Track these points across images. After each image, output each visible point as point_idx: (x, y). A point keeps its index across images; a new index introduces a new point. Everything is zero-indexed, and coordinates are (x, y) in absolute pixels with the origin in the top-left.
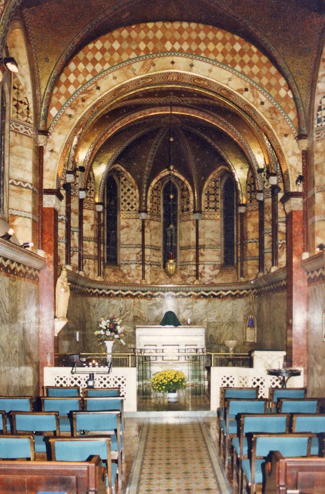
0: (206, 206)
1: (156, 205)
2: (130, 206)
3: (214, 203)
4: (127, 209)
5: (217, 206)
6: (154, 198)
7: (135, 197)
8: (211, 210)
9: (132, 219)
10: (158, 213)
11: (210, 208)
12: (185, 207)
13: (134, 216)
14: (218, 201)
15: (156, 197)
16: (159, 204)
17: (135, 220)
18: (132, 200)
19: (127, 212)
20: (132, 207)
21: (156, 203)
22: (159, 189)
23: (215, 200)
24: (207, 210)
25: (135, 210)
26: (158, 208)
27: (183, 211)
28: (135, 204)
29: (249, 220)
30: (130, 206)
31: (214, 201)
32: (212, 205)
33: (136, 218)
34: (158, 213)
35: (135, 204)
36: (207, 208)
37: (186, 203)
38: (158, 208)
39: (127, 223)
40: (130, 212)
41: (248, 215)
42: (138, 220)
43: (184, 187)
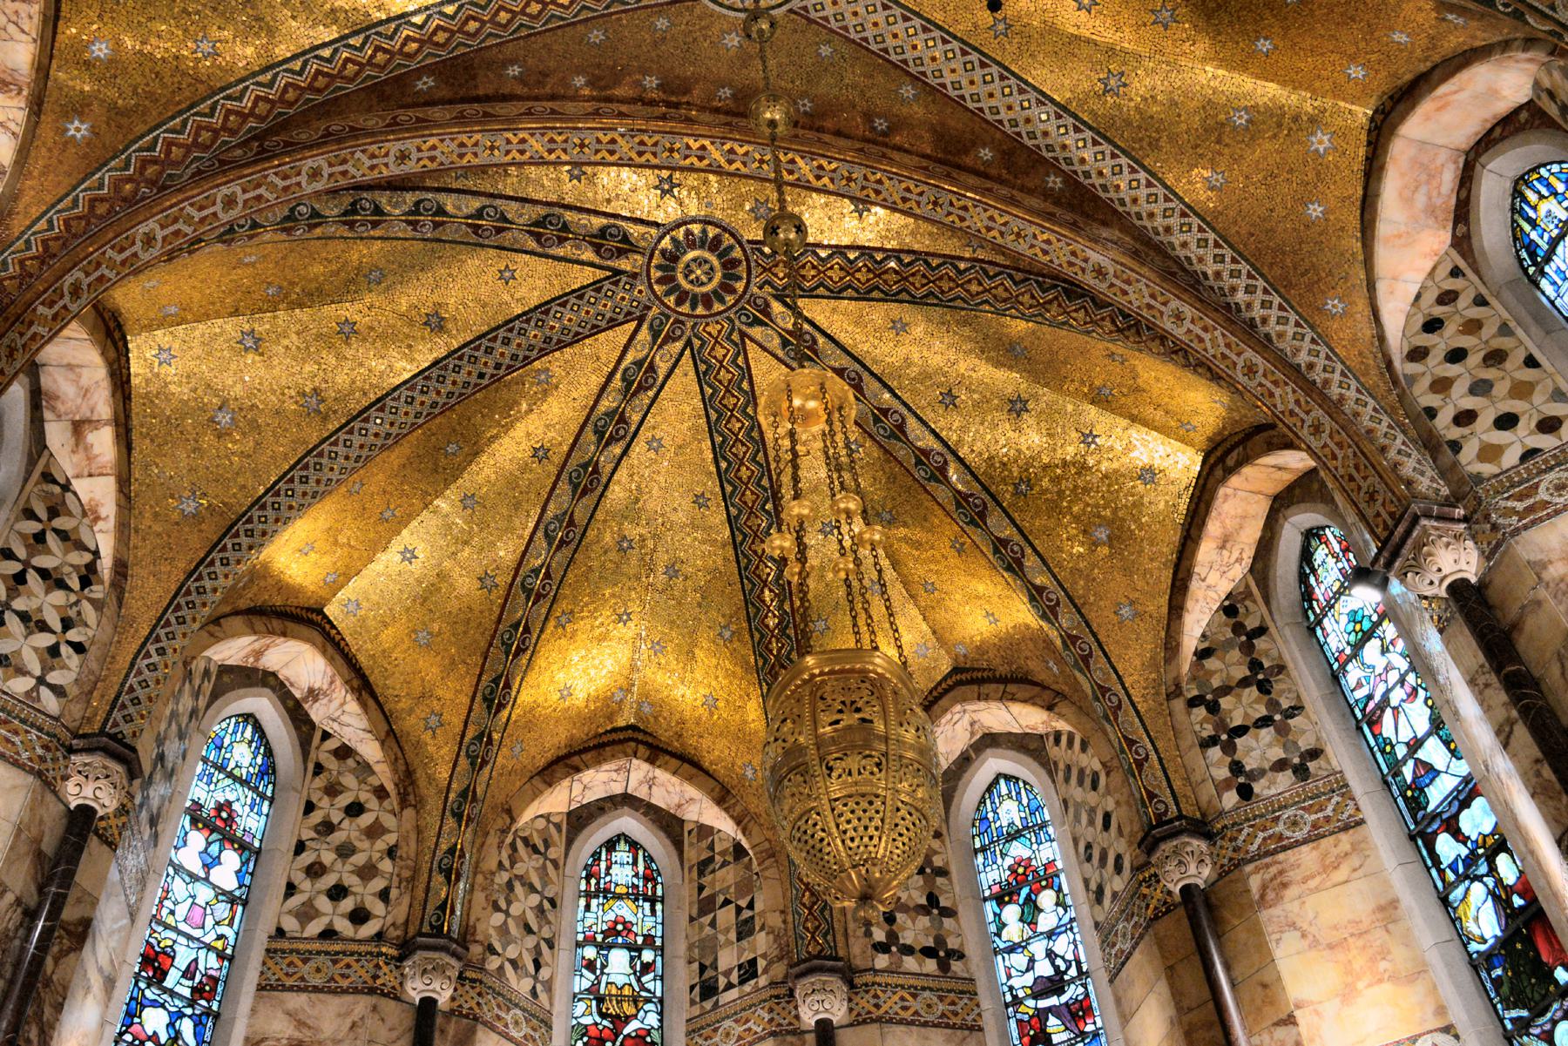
0: (879, 935)
1: (530, 941)
2: (348, 904)
3: (924, 921)
4: (315, 928)
5: (952, 943)
6: (518, 889)
7: (391, 852)
8: (910, 963)
9: (345, 991)
10: (534, 993)
11: (908, 950)
12: (728, 959)
13: (360, 973)
14: (949, 913)
15: (533, 889)
16: (551, 946)
17: (362, 1004)
18: (367, 872)
19: (317, 946)
20: (359, 916)
21: (528, 930)
22: (553, 853)
23: (932, 899)
24: (882, 961)
25: (379, 936)
26: (538, 965)
27: (708, 990)
28: (384, 895)
29: (1264, 915)
30: (348, 904)
31: (924, 910)
32: (914, 931)
33: (372, 991)
34: (534, 993)
35: (384, 895)
36: (882, 948)
37: (733, 936)
38: (537, 966)
39: (301, 1024)
40: (337, 947)
41: (1255, 883)
42: (388, 1006)
43: (711, 847)
